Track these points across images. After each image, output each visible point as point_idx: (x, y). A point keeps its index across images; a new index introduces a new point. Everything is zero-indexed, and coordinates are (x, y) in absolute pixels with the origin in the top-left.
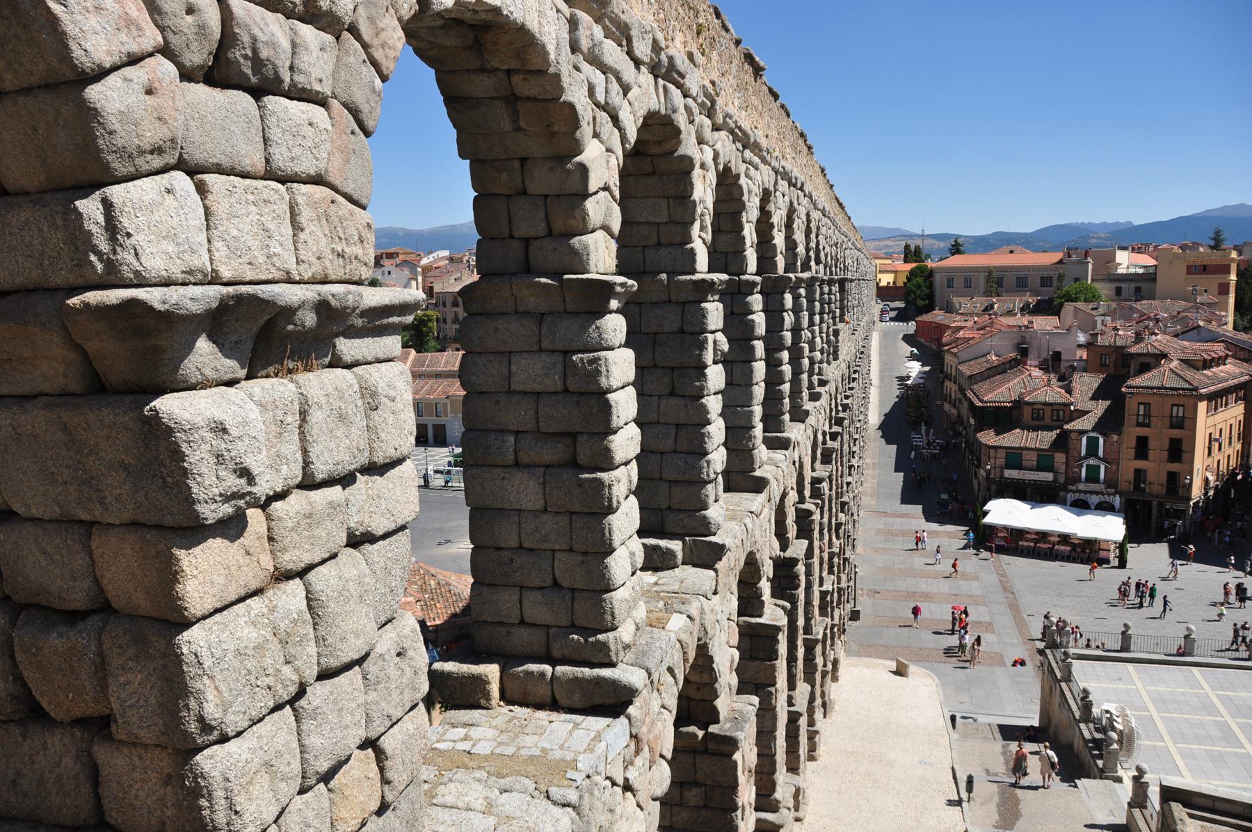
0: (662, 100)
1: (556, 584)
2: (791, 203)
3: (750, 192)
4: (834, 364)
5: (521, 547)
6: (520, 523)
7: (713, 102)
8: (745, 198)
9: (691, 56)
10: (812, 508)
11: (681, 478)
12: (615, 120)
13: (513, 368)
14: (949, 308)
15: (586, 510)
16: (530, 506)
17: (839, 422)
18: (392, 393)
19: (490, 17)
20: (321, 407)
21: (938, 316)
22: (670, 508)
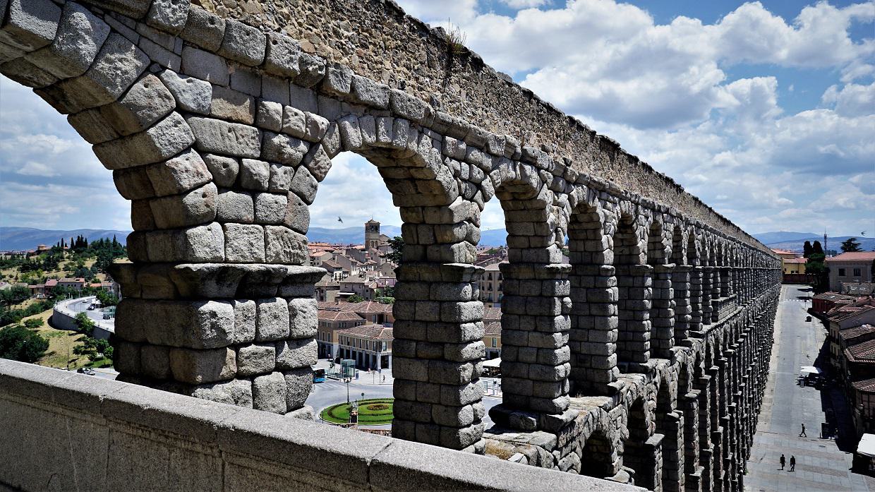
0: (518, 172)
1: (432, 422)
2: (655, 221)
3: (606, 216)
4: (713, 324)
5: (416, 401)
6: (416, 388)
7: (566, 170)
8: (602, 220)
9: (544, 148)
10: (676, 415)
11: (539, 378)
12: (479, 186)
13: (417, 309)
14: (839, 290)
15: (448, 383)
16: (421, 379)
17: (720, 364)
18: (305, 310)
19: (388, 146)
20: (266, 312)
21: (831, 296)
22: (533, 396)
